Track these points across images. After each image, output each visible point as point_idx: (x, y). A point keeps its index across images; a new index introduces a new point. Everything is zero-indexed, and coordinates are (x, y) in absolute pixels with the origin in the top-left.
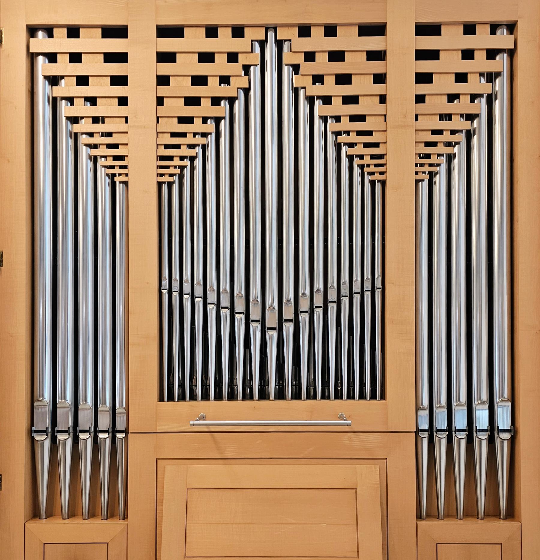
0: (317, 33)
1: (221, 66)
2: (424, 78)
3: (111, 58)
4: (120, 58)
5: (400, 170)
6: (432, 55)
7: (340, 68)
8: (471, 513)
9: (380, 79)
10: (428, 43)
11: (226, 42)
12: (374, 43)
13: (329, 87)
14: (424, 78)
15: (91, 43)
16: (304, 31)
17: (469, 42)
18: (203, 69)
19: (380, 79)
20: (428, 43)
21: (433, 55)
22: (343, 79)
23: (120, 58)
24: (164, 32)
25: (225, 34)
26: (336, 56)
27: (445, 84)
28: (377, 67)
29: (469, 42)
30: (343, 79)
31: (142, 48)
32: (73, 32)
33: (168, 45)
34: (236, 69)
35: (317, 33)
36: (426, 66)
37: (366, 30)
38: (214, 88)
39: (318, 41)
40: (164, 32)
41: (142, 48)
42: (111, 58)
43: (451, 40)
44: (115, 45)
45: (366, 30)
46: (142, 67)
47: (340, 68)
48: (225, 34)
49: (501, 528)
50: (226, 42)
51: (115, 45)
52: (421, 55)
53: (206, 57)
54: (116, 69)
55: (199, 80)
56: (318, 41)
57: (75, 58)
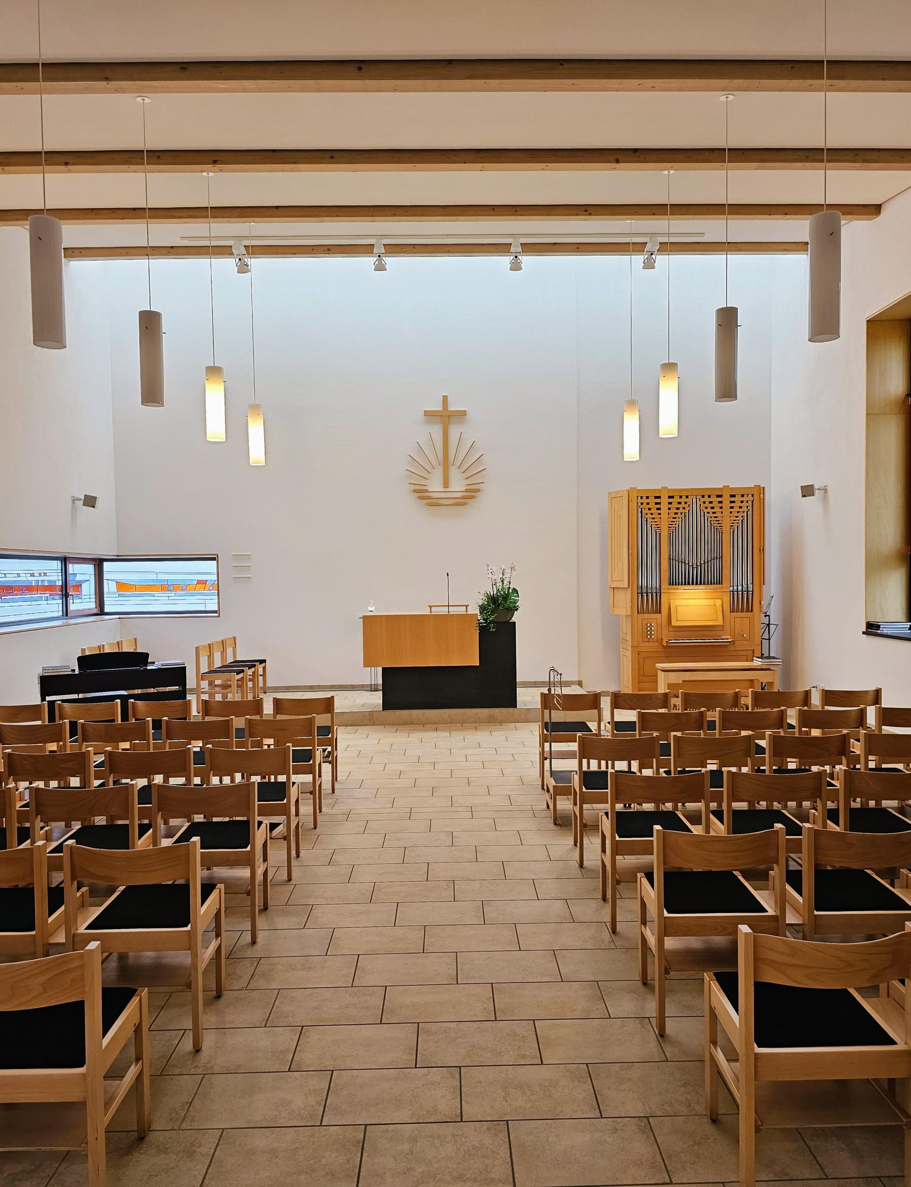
0: (706, 497)
1: (683, 505)
2: (732, 508)
3: (656, 504)
4: (659, 503)
5: (726, 529)
6: (734, 502)
7: (711, 505)
8: (742, 611)
9: (721, 508)
10: (733, 499)
11: (684, 500)
12: (720, 499)
13: (709, 510)
14: (732, 508)
15: (652, 501)
16: (703, 496)
17: (742, 499)
18: (678, 506)
19: (721, 508)
20: (733, 499)
21: (734, 502)
22: (712, 508)
23: (659, 503)
24: (670, 497)
25: (684, 497)
26: (711, 502)
27: (736, 509)
28: (721, 505)
29: (742, 499)
30: (712, 508)
31: (664, 501)
32: (647, 498)
33: (671, 500)
34: (686, 506)
35: (706, 497)
36: (732, 505)
37: (718, 496)
38: (681, 510)
39: (706, 499)
40: (670, 497)
41: (664, 501)
42: (656, 504)
43: (738, 499)
44: (658, 500)
45: (718, 496)
46: (664, 506)
47: (711, 505)
48: (684, 497)
49: (750, 614)
50: (684, 500)
51: (658, 500)
52: (731, 502)
53: (679, 503)
54: (658, 506)
55: (678, 509)
56: (706, 499)
57: (648, 504)
